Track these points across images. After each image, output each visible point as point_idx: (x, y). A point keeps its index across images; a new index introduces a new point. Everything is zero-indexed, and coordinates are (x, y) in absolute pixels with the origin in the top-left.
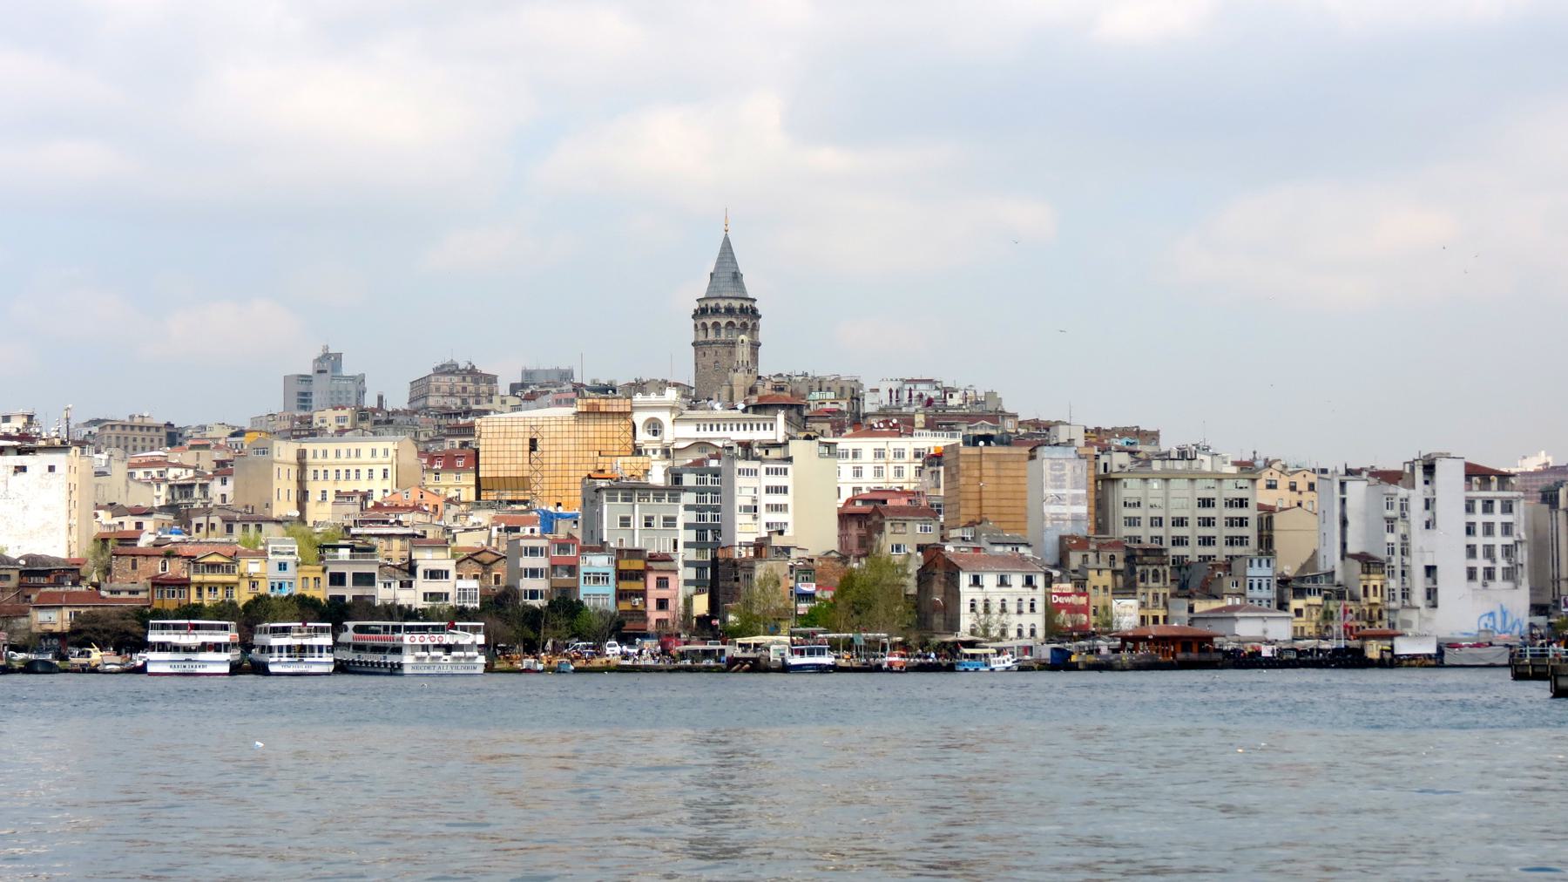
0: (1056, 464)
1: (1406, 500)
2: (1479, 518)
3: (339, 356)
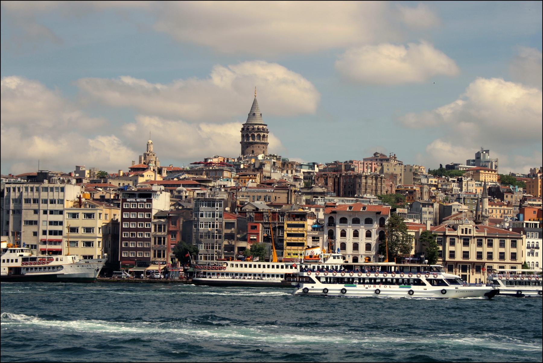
3: (487, 151)
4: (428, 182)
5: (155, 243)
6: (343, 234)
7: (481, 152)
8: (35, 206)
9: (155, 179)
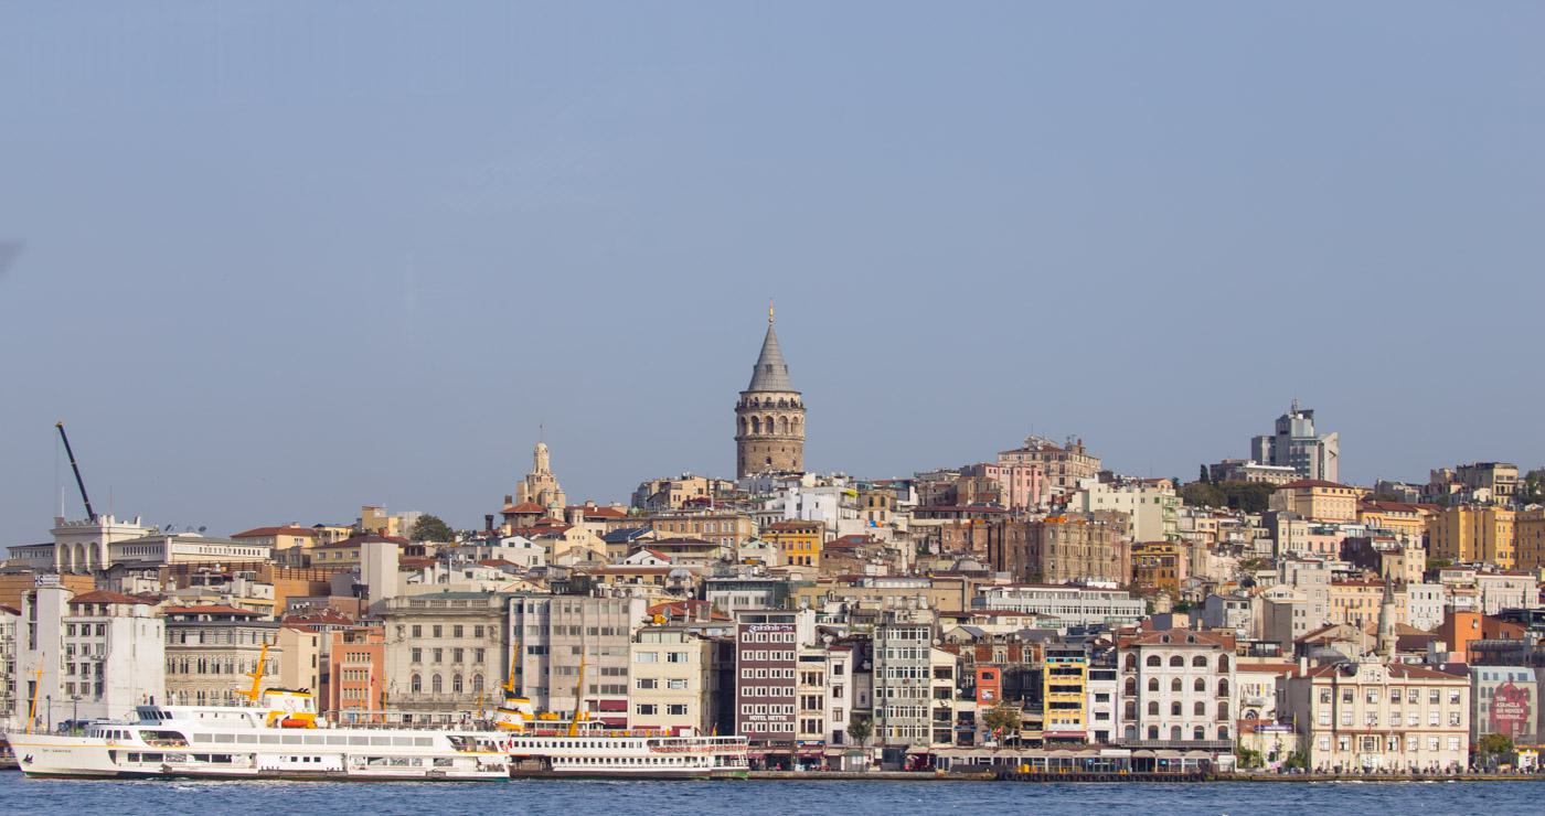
2: (79, 640)
3: (1308, 414)
4: (1194, 528)
5: (803, 707)
6: (1154, 686)
7: (1291, 416)
8: (576, 640)
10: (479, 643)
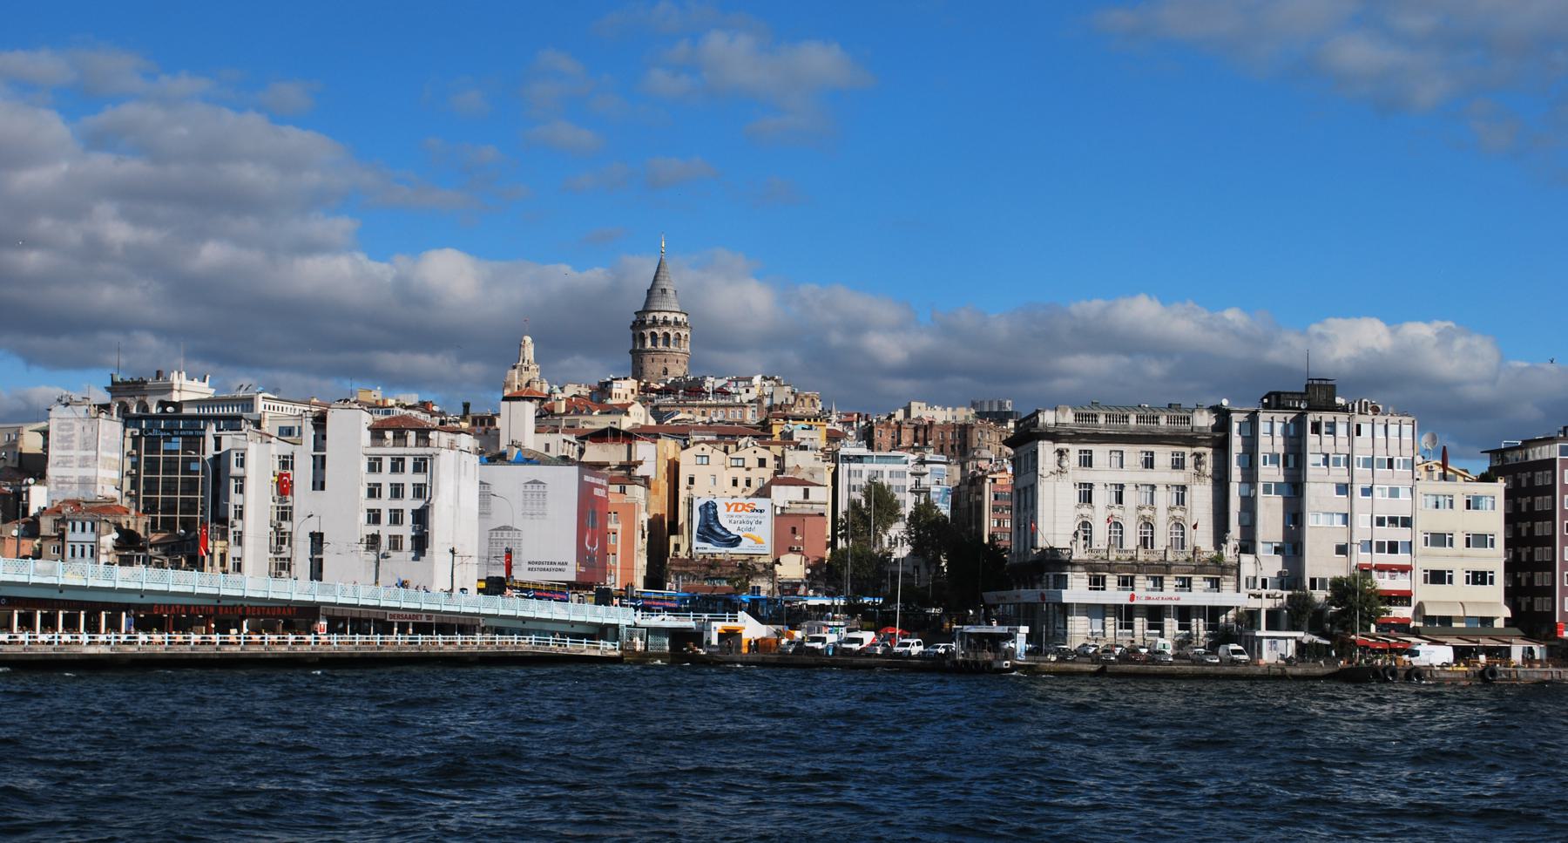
0: (63, 424)
1: (292, 457)
2: (386, 478)
9: (647, 421)
10: (1179, 477)
